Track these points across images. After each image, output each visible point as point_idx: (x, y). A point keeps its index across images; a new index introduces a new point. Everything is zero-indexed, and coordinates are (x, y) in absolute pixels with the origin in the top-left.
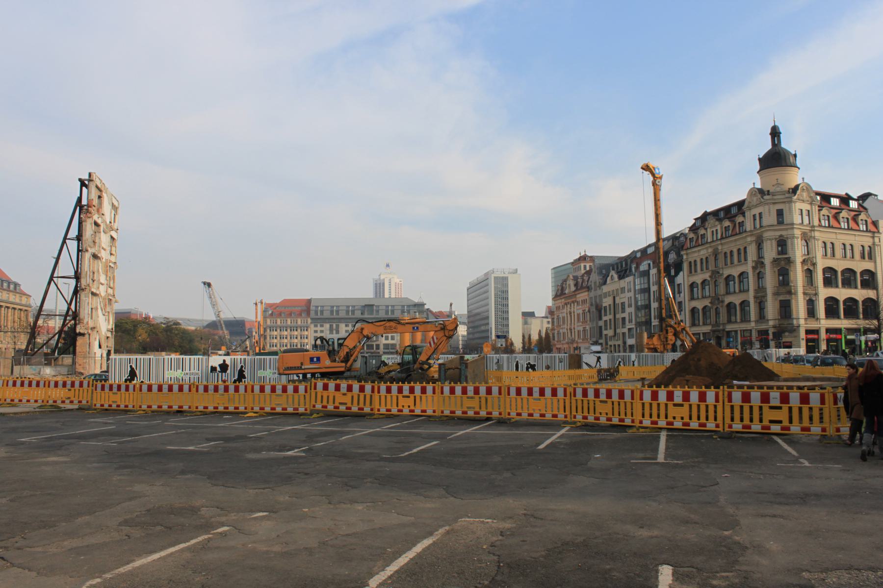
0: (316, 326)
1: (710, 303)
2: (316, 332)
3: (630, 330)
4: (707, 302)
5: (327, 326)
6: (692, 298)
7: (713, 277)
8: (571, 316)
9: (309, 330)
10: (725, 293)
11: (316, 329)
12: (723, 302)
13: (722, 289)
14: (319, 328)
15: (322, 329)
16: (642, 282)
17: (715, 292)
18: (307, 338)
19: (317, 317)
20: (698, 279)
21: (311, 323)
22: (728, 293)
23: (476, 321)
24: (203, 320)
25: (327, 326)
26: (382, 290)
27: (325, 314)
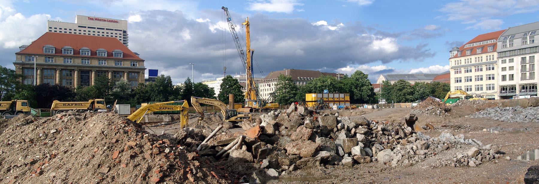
0: (504, 62)
2: (504, 69)
5: (518, 59)
11: (504, 65)
15: (511, 64)
18: (493, 78)
19: (506, 50)
25: (518, 59)
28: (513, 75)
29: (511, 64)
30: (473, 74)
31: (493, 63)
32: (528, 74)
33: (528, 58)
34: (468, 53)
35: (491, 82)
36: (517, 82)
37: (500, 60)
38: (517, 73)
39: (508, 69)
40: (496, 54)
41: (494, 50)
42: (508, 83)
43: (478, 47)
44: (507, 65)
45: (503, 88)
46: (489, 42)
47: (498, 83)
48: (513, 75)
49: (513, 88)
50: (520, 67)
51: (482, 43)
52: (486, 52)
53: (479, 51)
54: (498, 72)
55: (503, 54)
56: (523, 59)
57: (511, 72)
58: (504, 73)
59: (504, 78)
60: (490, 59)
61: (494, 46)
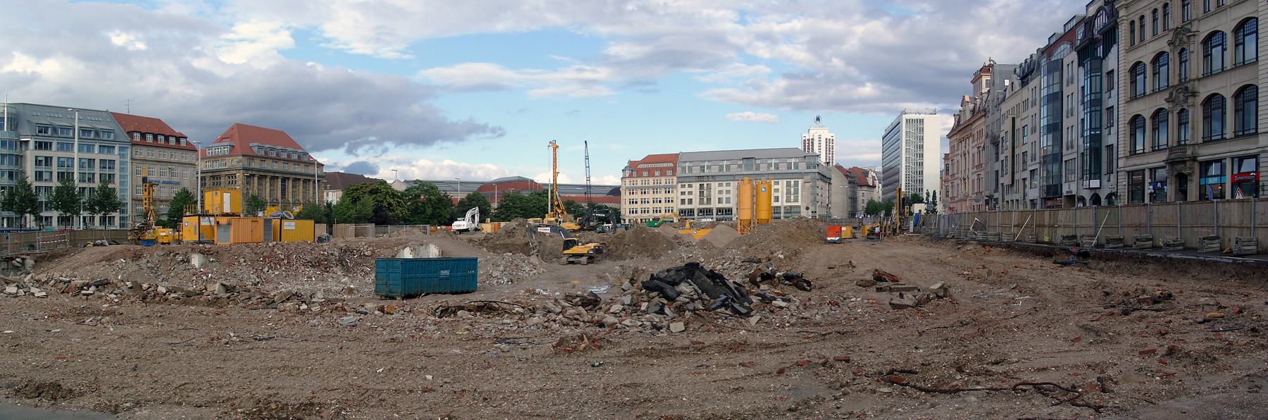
0: (683, 186)
1: (1167, 101)
2: (683, 193)
3: (1032, 172)
4: (1160, 102)
6: (1134, 98)
7: (1177, 43)
8: (966, 158)
9: (675, 191)
10: (1201, 76)
11: (683, 190)
12: (1194, 94)
13: (1196, 65)
14: (687, 189)
15: (690, 190)
16: (1051, 83)
17: (1180, 75)
18: (672, 201)
19: (685, 175)
20: (1146, 54)
21: (677, 183)
22: (1209, 75)
23: (890, 176)
24: (590, 187)
25: (696, 186)
26: (807, 145)
27: (694, 172)
28: (691, 199)
29: (690, 190)
30: (650, 196)
31: (672, 187)
32: (705, 200)
33: (705, 185)
34: (645, 174)
35: (670, 205)
36: (696, 205)
37: (680, 185)
38: (696, 198)
39: (687, 193)
40: (675, 178)
41: (674, 174)
42: (687, 206)
43: (657, 169)
44: (687, 189)
45: (682, 211)
46: (658, 165)
47: (677, 206)
48: (691, 199)
49: (691, 212)
50: (698, 193)
51: (650, 166)
52: (653, 176)
53: (645, 174)
54: (676, 195)
55: (682, 180)
56: (701, 186)
57: (690, 197)
58: (683, 197)
59: (683, 201)
60: (657, 183)
61: (674, 170)
